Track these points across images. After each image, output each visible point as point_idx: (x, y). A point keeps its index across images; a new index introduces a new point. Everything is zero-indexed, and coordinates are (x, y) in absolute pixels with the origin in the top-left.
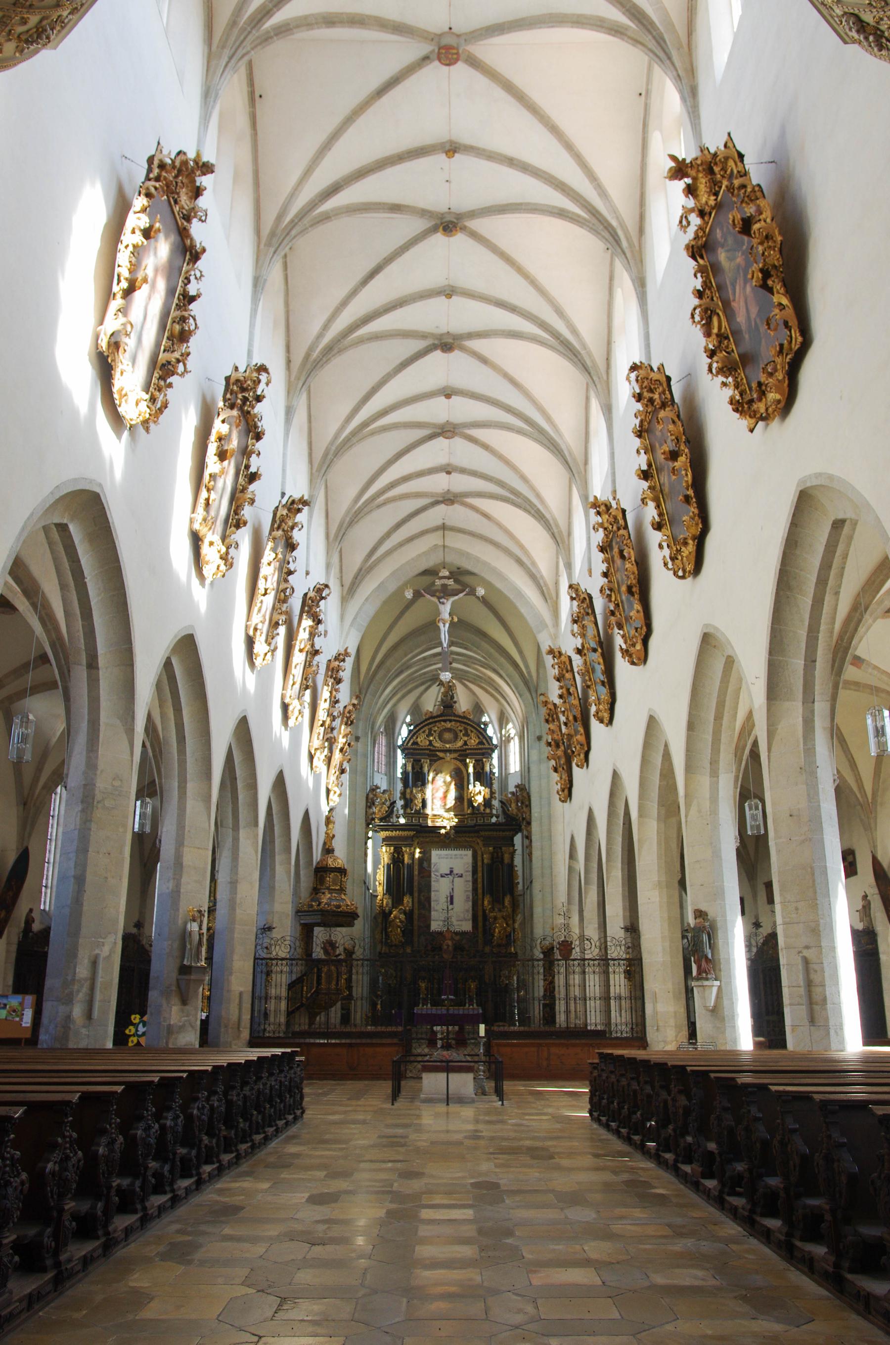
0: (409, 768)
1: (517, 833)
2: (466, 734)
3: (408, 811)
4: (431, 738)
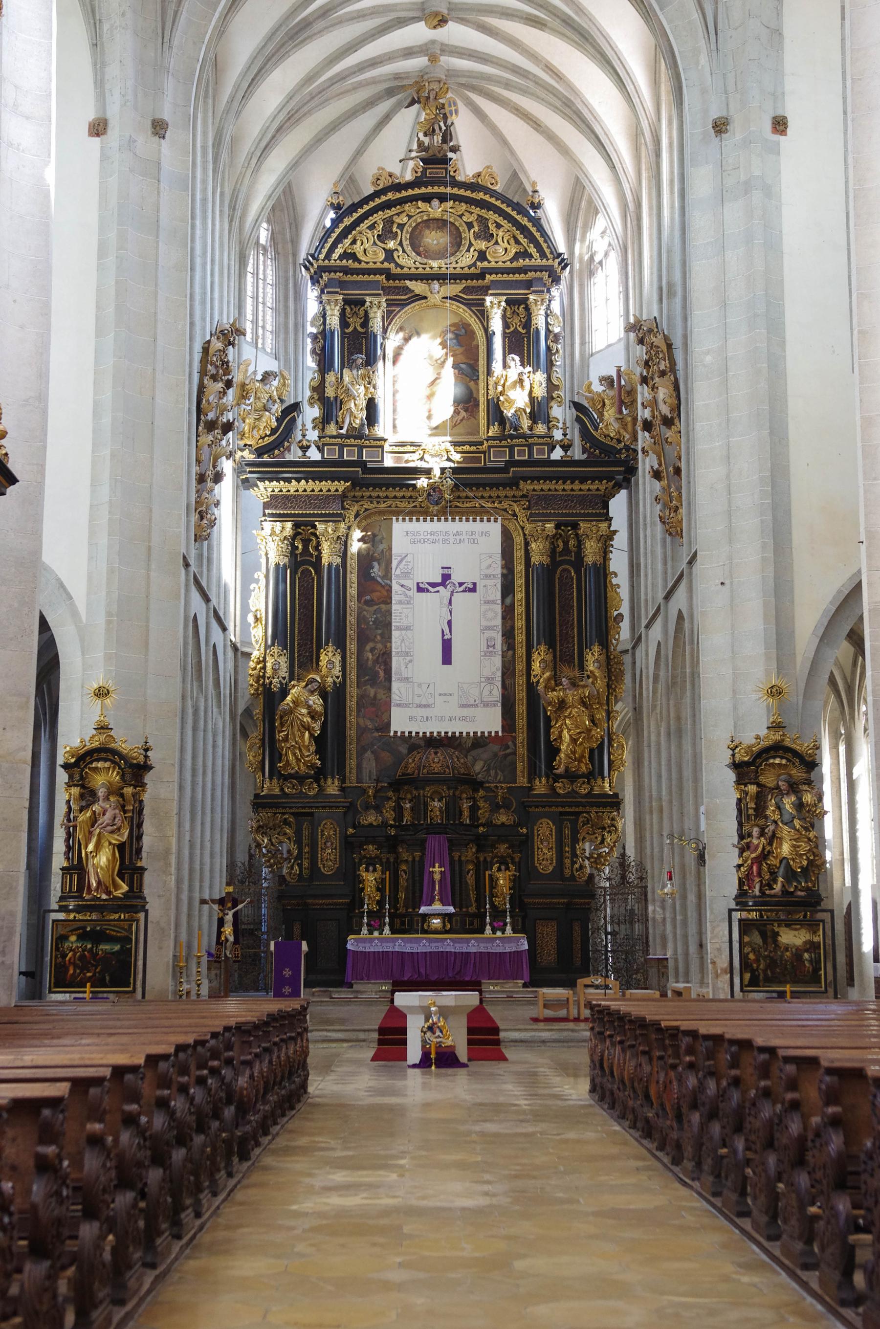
0: (334, 321)
1: (618, 487)
2: (486, 235)
3: (332, 429)
4: (391, 245)
